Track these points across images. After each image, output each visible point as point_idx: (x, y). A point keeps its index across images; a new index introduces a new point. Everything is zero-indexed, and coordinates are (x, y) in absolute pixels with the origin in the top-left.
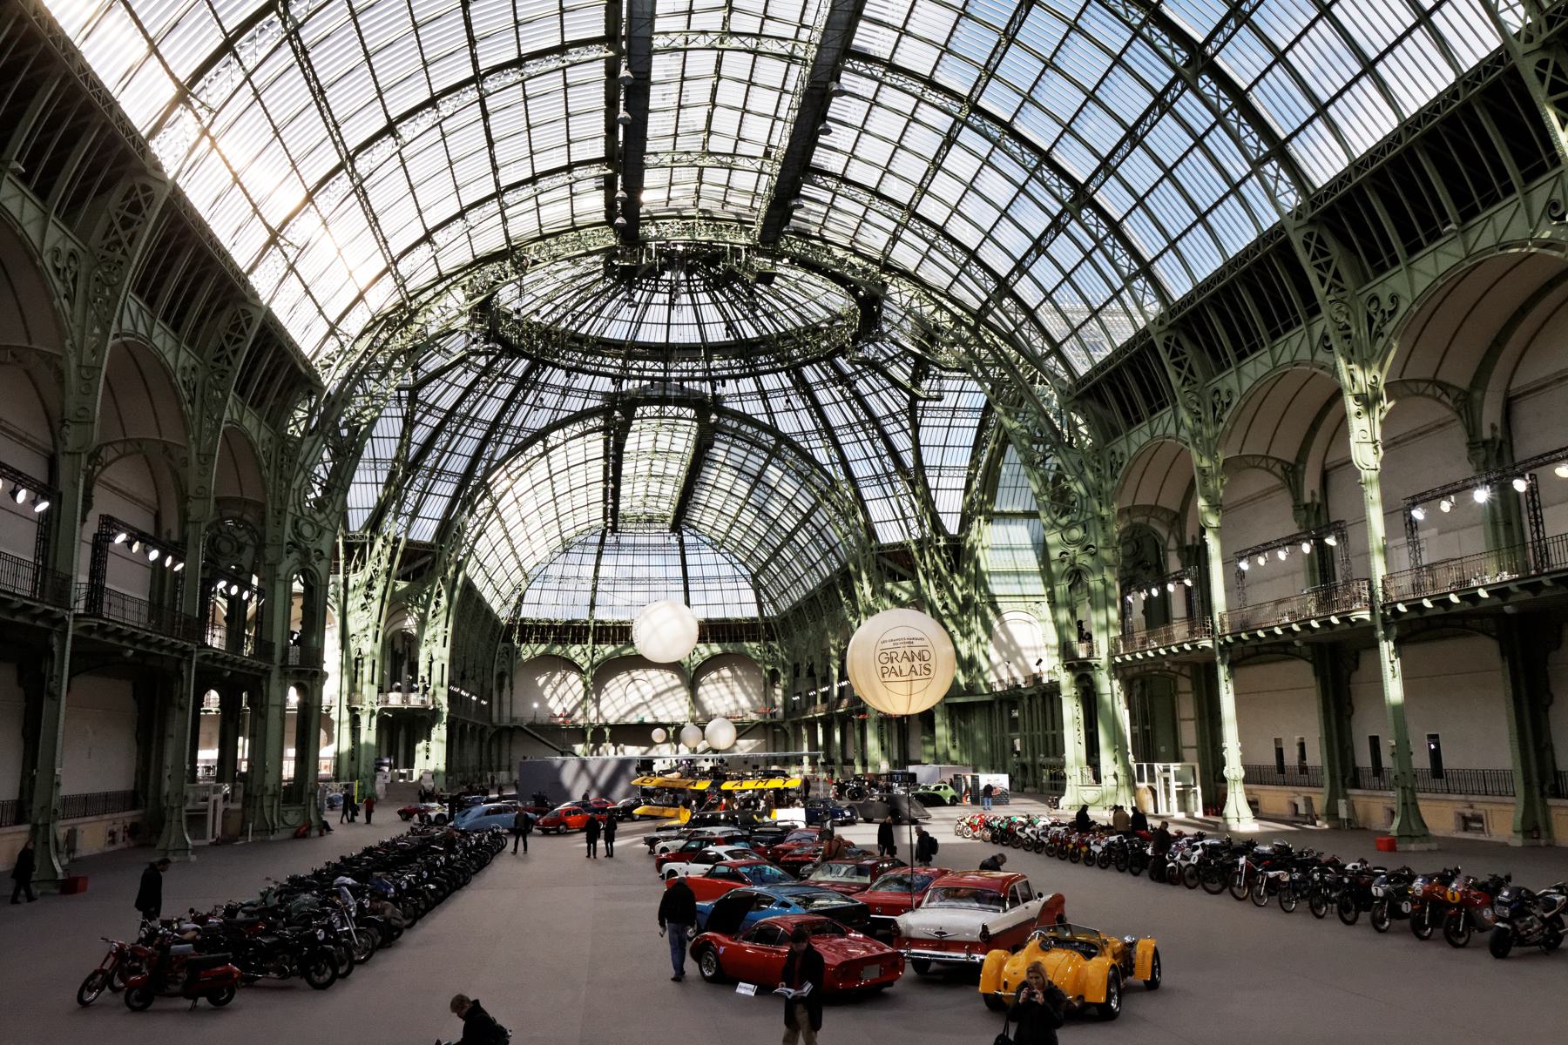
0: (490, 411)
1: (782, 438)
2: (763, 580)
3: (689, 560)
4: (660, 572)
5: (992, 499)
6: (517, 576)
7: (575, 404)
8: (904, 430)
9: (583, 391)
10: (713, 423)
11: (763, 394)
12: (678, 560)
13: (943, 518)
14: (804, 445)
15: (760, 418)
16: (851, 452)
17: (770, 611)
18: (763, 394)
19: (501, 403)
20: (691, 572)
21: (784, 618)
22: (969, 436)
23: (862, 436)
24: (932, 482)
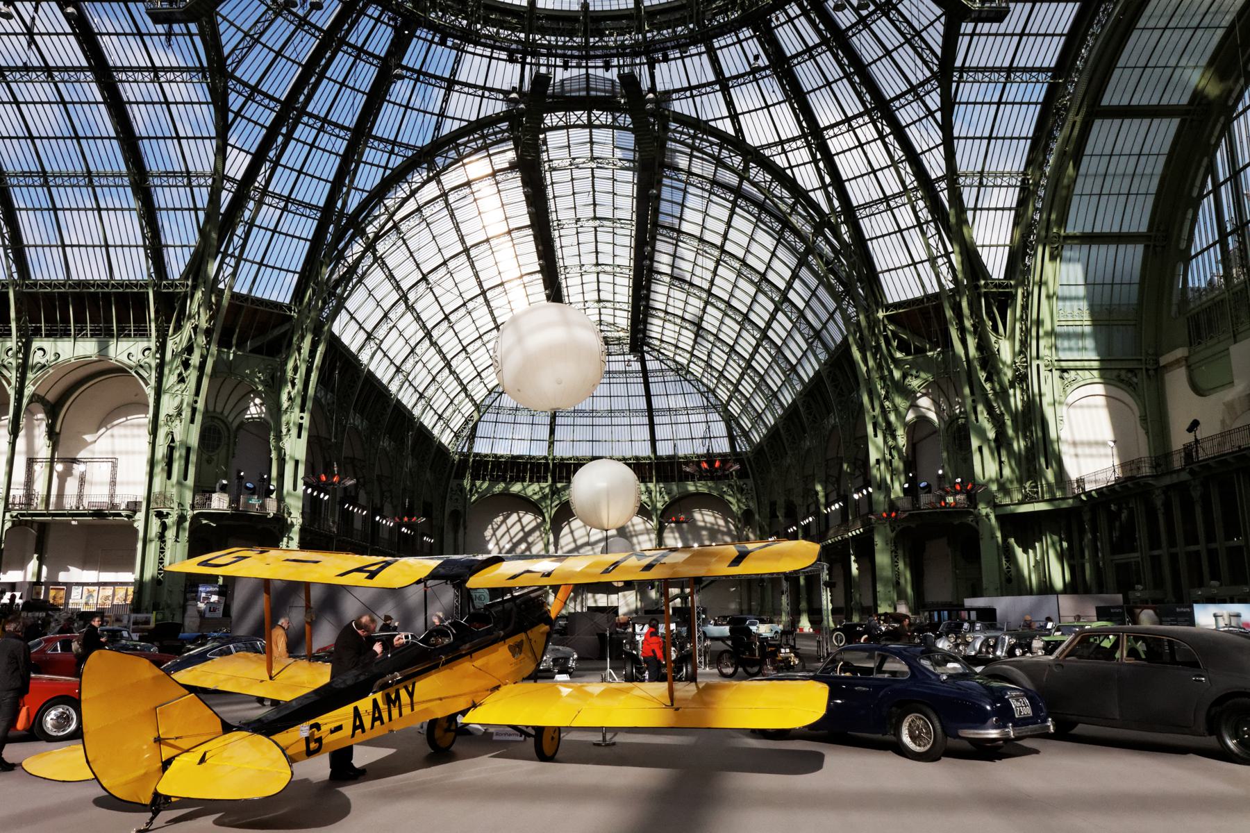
0: (348, 111)
1: (754, 155)
2: (735, 408)
3: (654, 389)
4: (619, 404)
5: (1063, 221)
6: (468, 408)
7: (464, 108)
8: (931, 113)
9: (475, 86)
10: (655, 137)
11: (723, 83)
12: (640, 389)
13: (984, 254)
14: (780, 161)
15: (720, 125)
16: (848, 165)
17: (742, 446)
18: (723, 83)
19: (361, 100)
20: (657, 403)
21: (758, 450)
22: (1024, 121)
23: (867, 132)
24: (968, 197)
